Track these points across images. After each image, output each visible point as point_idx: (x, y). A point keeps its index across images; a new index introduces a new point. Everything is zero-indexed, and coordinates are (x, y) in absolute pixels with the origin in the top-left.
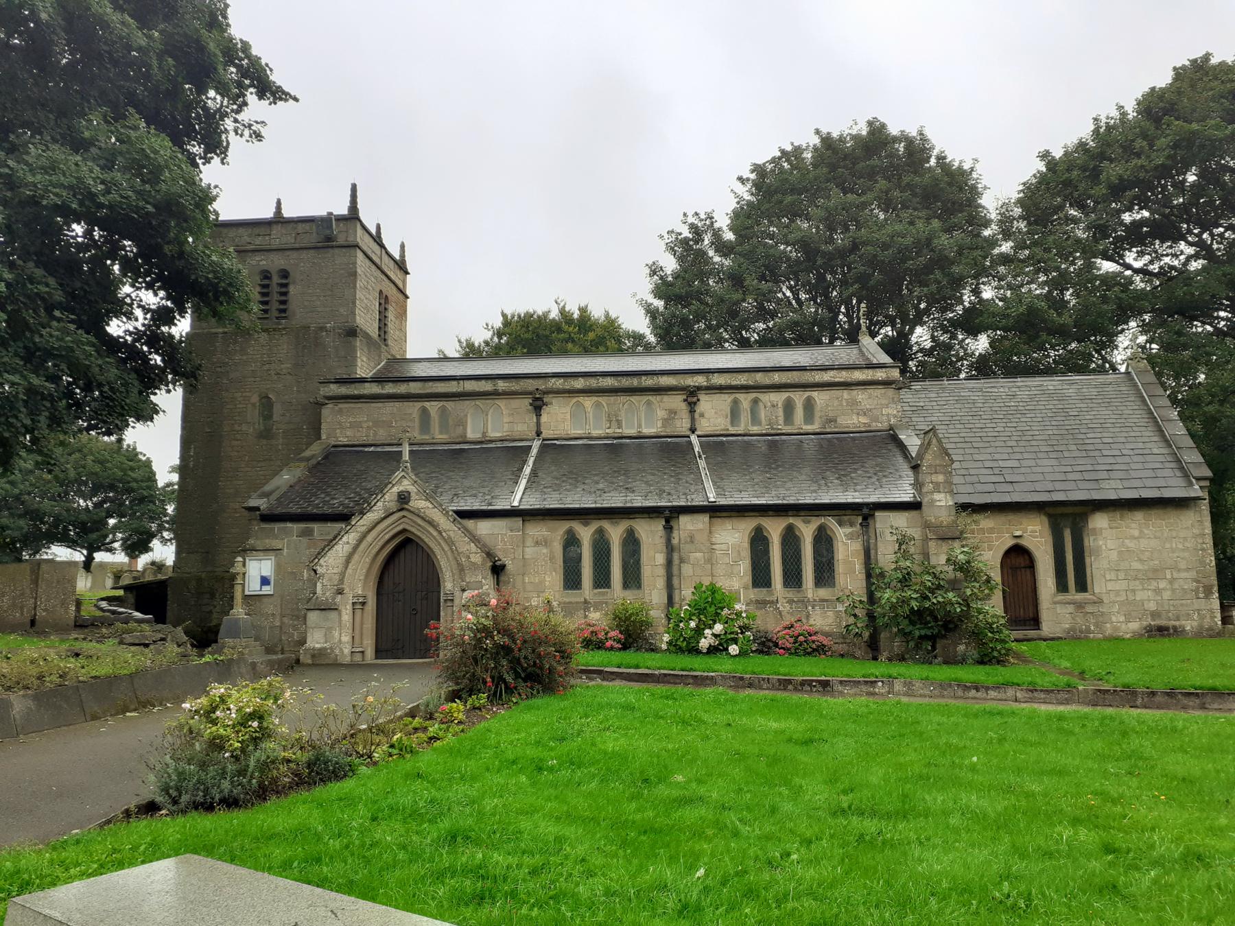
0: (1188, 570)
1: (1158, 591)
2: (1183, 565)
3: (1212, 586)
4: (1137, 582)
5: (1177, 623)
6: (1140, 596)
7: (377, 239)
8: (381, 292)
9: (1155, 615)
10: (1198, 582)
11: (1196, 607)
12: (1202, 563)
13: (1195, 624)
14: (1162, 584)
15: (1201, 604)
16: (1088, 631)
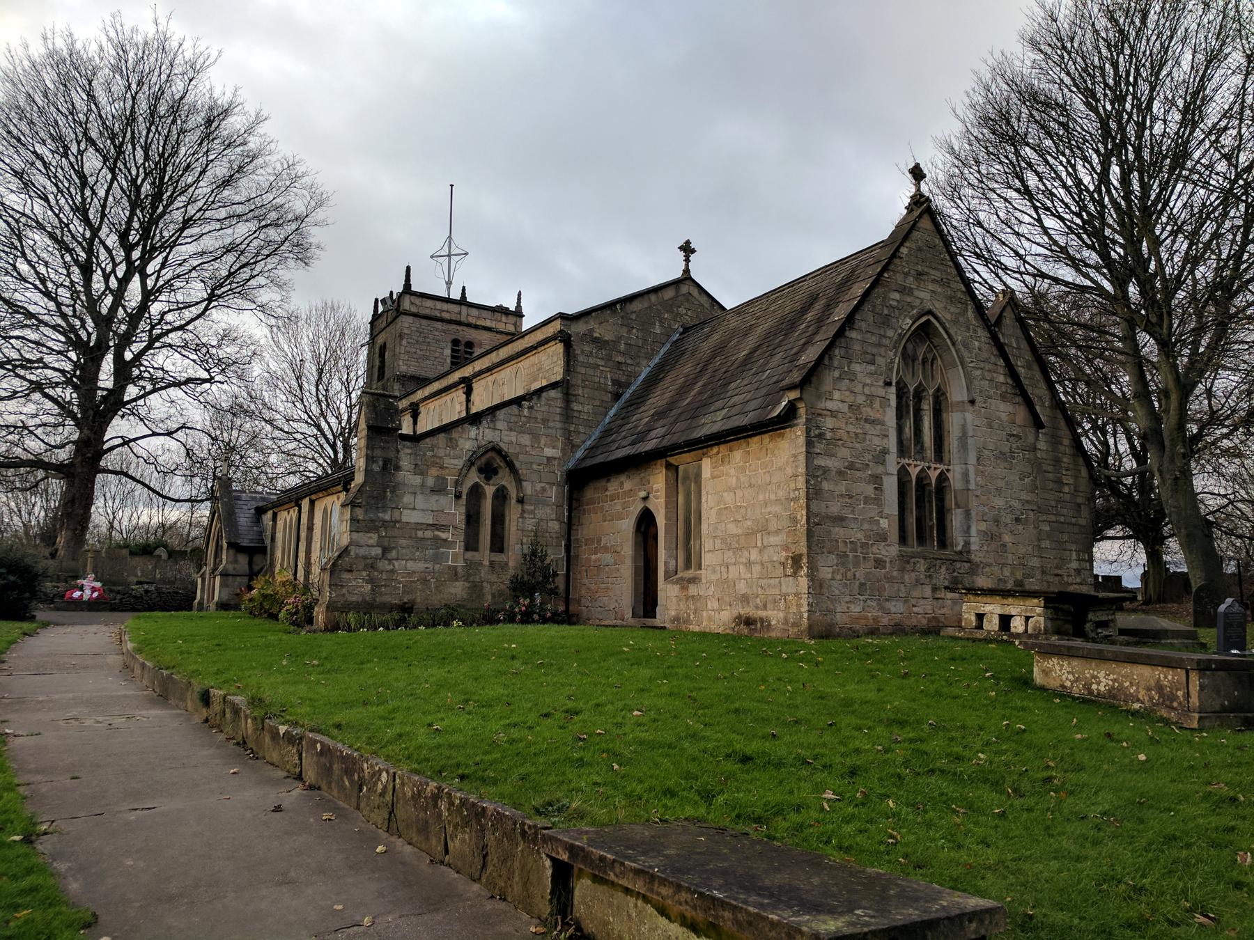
0: (778, 532)
1: (749, 564)
2: (773, 526)
3: (801, 555)
4: (730, 553)
5: (763, 614)
6: (734, 572)
7: (463, 301)
8: (455, 342)
9: (745, 599)
10: (787, 548)
11: (784, 590)
12: (794, 520)
13: (781, 615)
14: (754, 555)
15: (788, 586)
16: (688, 621)
